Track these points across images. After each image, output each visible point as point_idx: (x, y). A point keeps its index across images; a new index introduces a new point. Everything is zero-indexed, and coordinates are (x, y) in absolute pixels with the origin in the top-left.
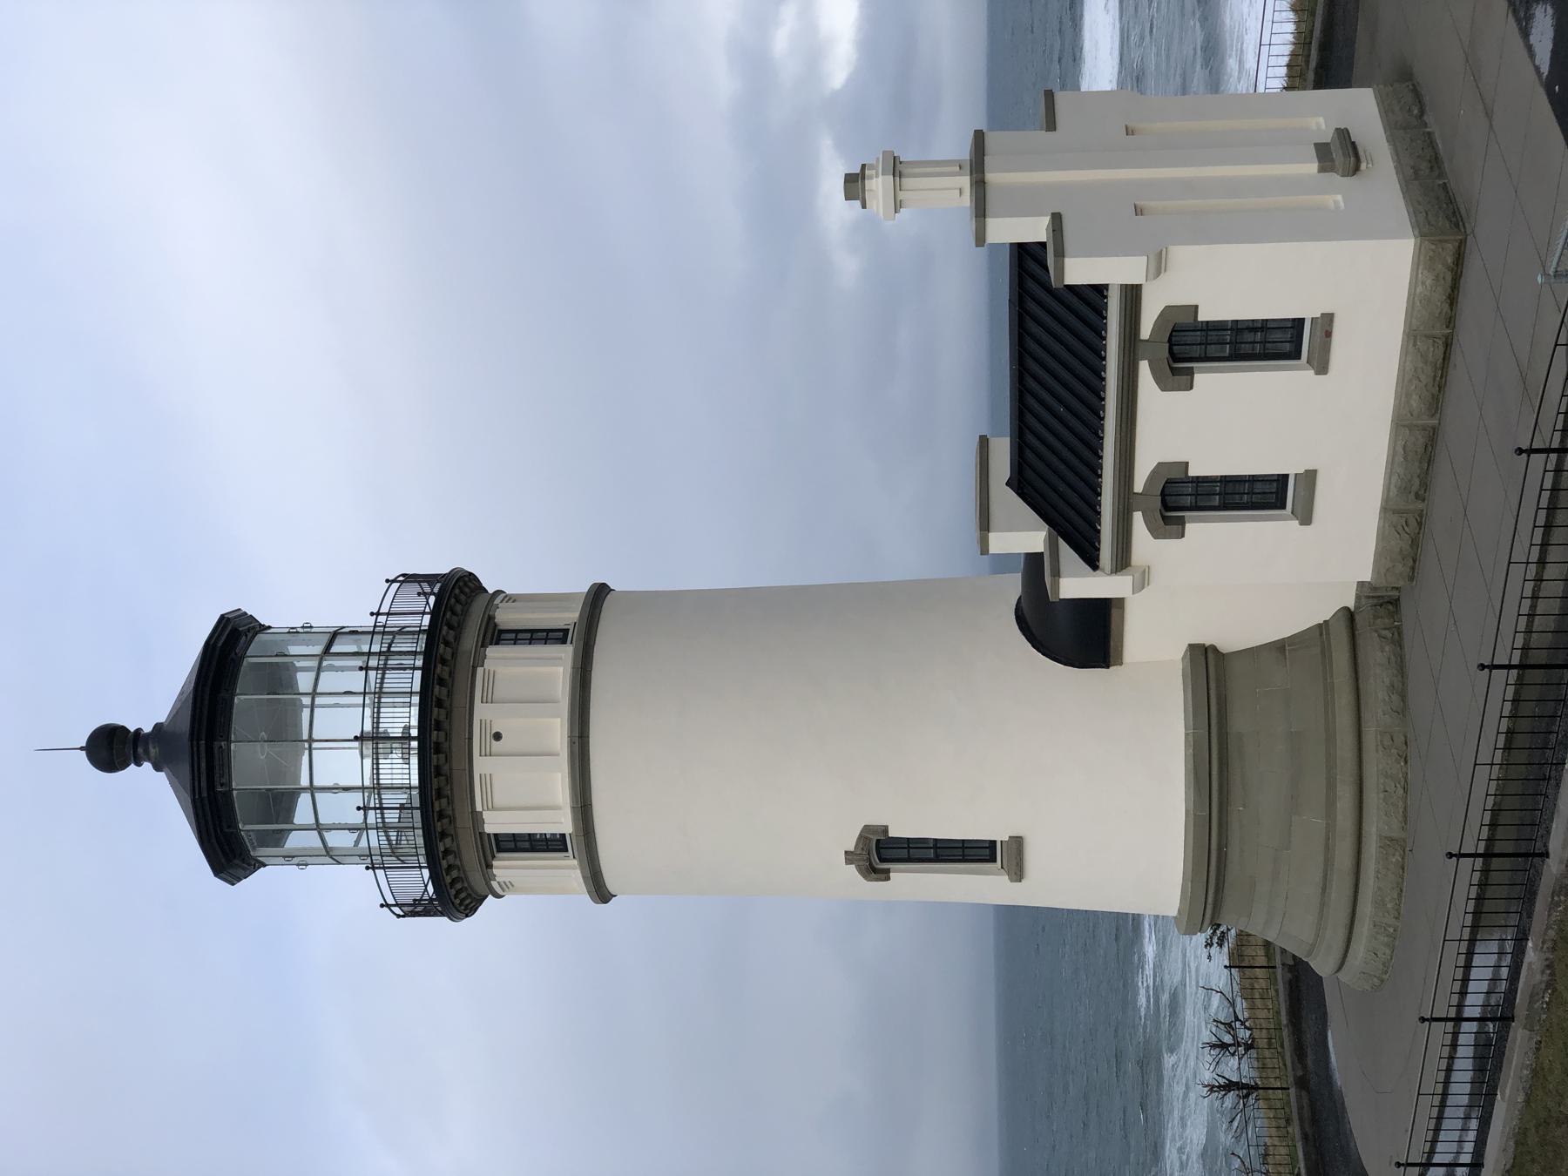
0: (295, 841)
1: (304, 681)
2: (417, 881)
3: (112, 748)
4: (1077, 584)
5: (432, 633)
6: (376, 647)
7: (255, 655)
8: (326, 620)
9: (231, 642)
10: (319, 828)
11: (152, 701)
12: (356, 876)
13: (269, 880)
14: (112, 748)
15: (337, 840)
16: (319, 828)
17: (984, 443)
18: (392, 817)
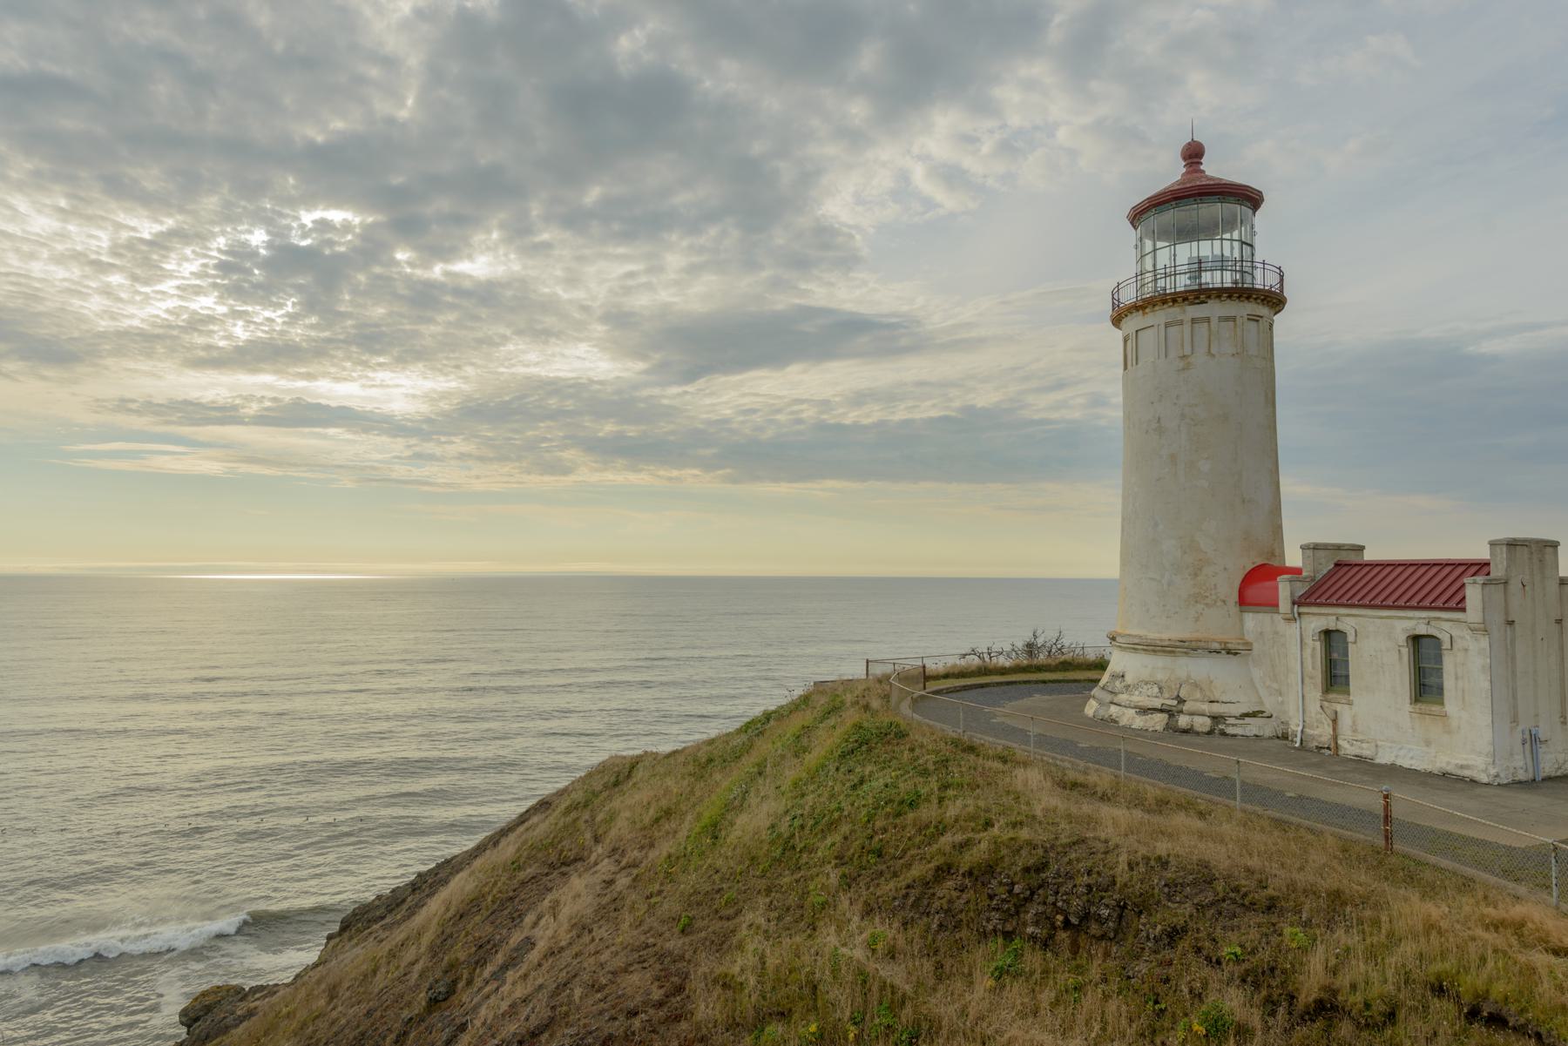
0: (1149, 245)
1: (1227, 236)
2: (1129, 296)
3: (1194, 154)
4: (1284, 590)
5: (1253, 290)
6: (1245, 265)
7: (1239, 210)
8: (1258, 242)
9: (1251, 199)
10: (1155, 250)
11: (1214, 168)
12: (1133, 269)
13: (1132, 235)
14: (1194, 154)
15: (1148, 261)
16: (1155, 250)
17: (1361, 548)
18: (1161, 283)
